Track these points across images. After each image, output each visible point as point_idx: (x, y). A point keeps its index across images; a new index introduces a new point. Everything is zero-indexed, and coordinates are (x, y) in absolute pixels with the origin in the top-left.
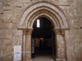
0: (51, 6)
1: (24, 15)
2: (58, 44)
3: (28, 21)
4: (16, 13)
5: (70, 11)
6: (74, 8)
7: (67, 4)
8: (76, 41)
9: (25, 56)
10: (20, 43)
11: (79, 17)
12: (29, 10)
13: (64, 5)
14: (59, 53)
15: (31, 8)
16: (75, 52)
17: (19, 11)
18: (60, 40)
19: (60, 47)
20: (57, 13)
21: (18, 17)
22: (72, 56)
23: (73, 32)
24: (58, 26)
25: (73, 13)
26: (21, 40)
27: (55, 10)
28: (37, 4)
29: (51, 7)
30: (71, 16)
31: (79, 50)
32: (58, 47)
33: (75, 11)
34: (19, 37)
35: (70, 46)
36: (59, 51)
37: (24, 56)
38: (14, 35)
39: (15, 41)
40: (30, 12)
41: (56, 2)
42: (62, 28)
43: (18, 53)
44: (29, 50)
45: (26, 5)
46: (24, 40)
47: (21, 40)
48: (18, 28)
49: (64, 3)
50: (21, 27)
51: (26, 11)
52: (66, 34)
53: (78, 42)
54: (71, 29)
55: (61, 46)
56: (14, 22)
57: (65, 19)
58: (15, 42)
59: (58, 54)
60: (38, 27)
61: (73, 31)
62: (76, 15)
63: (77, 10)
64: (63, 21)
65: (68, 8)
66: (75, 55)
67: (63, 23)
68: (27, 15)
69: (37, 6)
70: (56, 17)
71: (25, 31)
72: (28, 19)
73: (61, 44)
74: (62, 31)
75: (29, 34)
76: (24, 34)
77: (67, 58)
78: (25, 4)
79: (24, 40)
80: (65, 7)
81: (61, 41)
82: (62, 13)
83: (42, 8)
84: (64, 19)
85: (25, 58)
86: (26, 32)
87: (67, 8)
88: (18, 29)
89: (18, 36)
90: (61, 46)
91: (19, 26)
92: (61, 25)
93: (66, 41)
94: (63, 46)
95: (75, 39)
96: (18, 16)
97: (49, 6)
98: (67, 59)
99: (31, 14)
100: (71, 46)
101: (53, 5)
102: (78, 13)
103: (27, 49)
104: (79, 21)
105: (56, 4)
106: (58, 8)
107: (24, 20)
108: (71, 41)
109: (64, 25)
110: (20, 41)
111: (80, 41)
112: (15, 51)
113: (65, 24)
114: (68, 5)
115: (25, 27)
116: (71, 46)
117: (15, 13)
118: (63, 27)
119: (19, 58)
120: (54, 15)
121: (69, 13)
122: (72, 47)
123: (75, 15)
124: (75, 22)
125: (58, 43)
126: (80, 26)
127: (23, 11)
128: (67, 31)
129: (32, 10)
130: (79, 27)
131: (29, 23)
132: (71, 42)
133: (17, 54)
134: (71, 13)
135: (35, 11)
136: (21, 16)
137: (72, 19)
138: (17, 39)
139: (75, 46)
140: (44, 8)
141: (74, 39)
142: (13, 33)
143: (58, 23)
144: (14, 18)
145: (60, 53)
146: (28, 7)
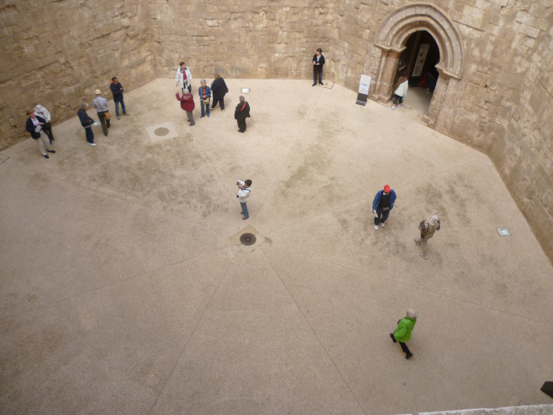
0: (442, 21)
3: (395, 36)
5: (478, 45)
6: (491, 41)
7: (480, 24)
8: (462, 105)
11: (492, 64)
12: (399, 16)
13: (470, 24)
15: (404, 12)
19: (437, 99)
20: (449, 39)
22: (445, 123)
23: (466, 87)
25: (481, 52)
28: (417, 8)
29: (441, 23)
30: (473, 57)
31: (461, 120)
32: (434, 98)
33: (489, 47)
40: (402, 20)
41: (457, 12)
43: (366, 85)
44: (387, 82)
46: (382, 65)
47: (377, 64)
49: (473, 21)
51: (394, 17)
53: (465, 108)
61: (466, 85)
62: (487, 56)
63: (496, 47)
65: (477, 35)
69: (415, 11)
72: (394, 32)
73: (440, 96)
79: (382, 65)
80: (471, 29)
82: (457, 43)
87: (476, 34)
95: (463, 100)
99: (396, 29)
100: (450, 108)
102: (494, 54)
104: (489, 72)
108: (453, 101)
111: (471, 108)
112: (362, 81)
114: (479, 28)
116: (450, 108)
119: (422, 47)
121: (473, 48)
122: (452, 110)
123: (484, 55)
124: (478, 71)
126: (486, 82)
128: (454, 80)
129: (404, 16)
130: (482, 83)
133: (364, 86)
134: (478, 49)
136: (384, 24)
137: (475, 62)
139: (458, 112)
141: (461, 99)
144: (373, 23)
145: (433, 109)
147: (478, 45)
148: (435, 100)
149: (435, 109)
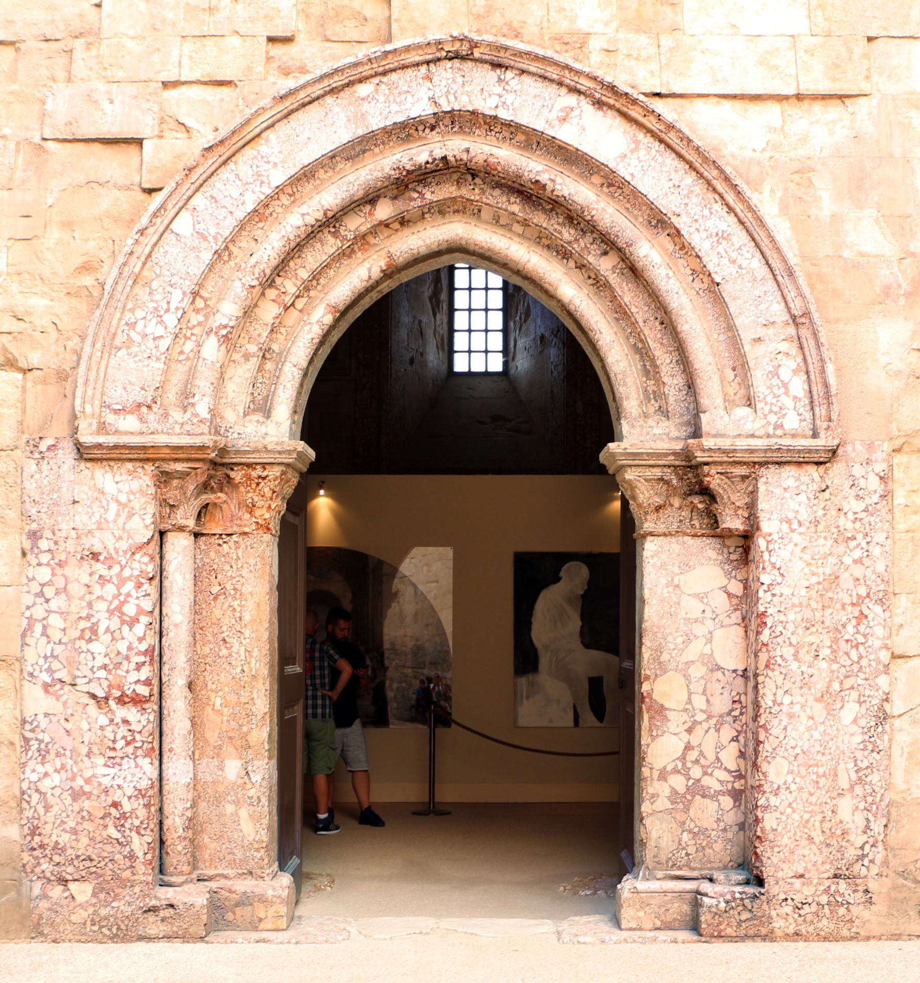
1: (170, 251)
2: (663, 668)
4: (68, 225)
9: (192, 824)
10: (122, 647)
12: (239, 188)
14: (663, 803)
15: (273, 144)
16: (888, 787)
17: (107, 200)
18: (693, 608)
20: (659, 222)
21: (88, 280)
24: (663, 412)
26: (130, 610)
27: (624, 172)
28: (363, 89)
29: (567, 135)
32: (661, 710)
34: (100, 568)
35: (818, 707)
36: (663, 775)
37: (175, 822)
38: (34, 536)
39: (55, 621)
41: (643, 41)
42: (708, 442)
45: (207, 116)
47: (141, 601)
48: (87, 438)
50: (129, 423)
51: (199, 200)
52: (765, 526)
54: (854, 450)
55: (699, 702)
56: (35, 358)
57: (777, 310)
58: (56, 635)
59: (645, 808)
64: (746, 336)
66: (877, 827)
67: (741, 366)
68: (207, 256)
70: (633, 271)
71: (183, 475)
73: (697, 672)
74: (715, 482)
75: (248, 522)
76: (181, 529)
77: (768, 872)
78: (188, 103)
79: (178, 610)
81: (700, 630)
83: (421, 153)
84: (755, 305)
85: (194, 845)
86: (205, 487)
88: (85, 454)
89: (97, 548)
90: (699, 702)
91: (110, 418)
92: (712, 390)
93: (765, 636)
94: (722, 704)
96: (86, 268)
97: (526, 119)
98: (760, 882)
100: (830, 699)
101: (599, 104)
103: (212, 737)
105: (635, 77)
106: (664, 136)
107: (171, 320)
109: (750, 402)
110: (115, 623)
113: (760, 386)
115: (177, 430)
117: (54, 235)
118: (729, 427)
120: (609, 243)
125: (659, 650)
127: (159, 198)
128: (789, 475)
131: (241, 374)
132: (836, 641)
135: (330, 195)
138: (76, 589)
139: (896, 707)
140: (454, 146)
142: (25, 516)
143: (664, 359)
144: (38, 303)
146: (228, 148)
147: (857, 186)
148: (676, 721)
149: (697, 790)
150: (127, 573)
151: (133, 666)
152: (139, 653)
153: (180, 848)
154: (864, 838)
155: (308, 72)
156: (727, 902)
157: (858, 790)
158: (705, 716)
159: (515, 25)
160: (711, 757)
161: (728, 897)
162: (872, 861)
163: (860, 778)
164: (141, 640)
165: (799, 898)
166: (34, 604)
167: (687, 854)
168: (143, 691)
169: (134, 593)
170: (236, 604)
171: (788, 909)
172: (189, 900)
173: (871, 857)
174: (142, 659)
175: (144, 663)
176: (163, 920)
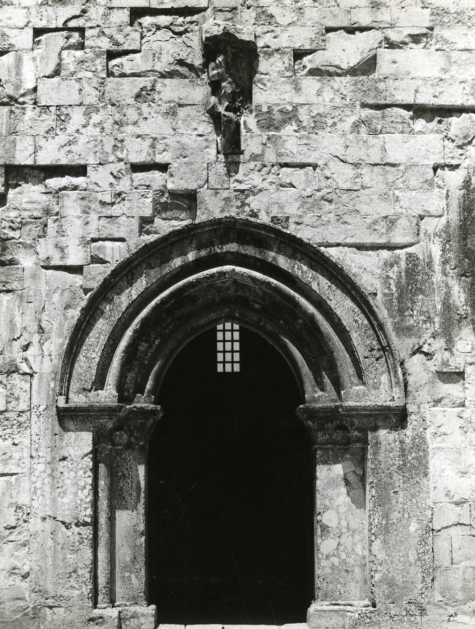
26: (82, 483)
60: (228, 368)
82: (349, 303)
150: (80, 466)
151: (83, 509)
152: (86, 503)
153: (104, 591)
154: (422, 585)
155: (158, 233)
156: (359, 615)
157: (418, 563)
158: (347, 530)
159: (255, 211)
160: (350, 549)
161: (360, 612)
162: (426, 596)
163: (419, 558)
164: (86, 497)
165: (393, 612)
166: (37, 481)
167: (340, 594)
168: (89, 520)
169: (83, 476)
170: (129, 481)
171: (387, 618)
172: (110, 615)
173: (426, 594)
174: (87, 506)
175: (88, 508)
176: (97, 624)
